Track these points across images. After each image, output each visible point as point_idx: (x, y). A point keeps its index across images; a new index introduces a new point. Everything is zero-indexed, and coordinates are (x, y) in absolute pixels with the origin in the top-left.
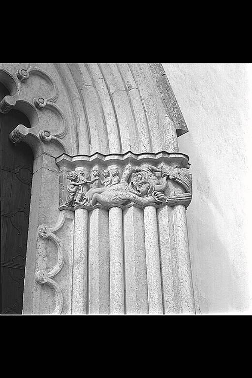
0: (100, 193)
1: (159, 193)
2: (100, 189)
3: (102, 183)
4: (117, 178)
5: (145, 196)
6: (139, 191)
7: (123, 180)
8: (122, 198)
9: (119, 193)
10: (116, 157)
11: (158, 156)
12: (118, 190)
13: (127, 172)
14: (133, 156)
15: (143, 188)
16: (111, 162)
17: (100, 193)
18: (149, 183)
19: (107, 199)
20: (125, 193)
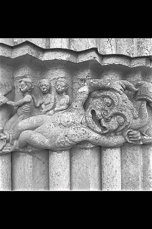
0: (33, 129)
1: (135, 132)
2: (33, 120)
3: (38, 105)
4: (66, 98)
5: (113, 134)
6: (104, 128)
7: (78, 104)
8: (76, 141)
9: (71, 131)
10: (65, 57)
11: (135, 64)
12: (68, 125)
13: (85, 89)
14: (98, 59)
15: (113, 124)
16: (55, 64)
17: (33, 129)
18: (124, 117)
19: (47, 142)
20: (80, 131)
